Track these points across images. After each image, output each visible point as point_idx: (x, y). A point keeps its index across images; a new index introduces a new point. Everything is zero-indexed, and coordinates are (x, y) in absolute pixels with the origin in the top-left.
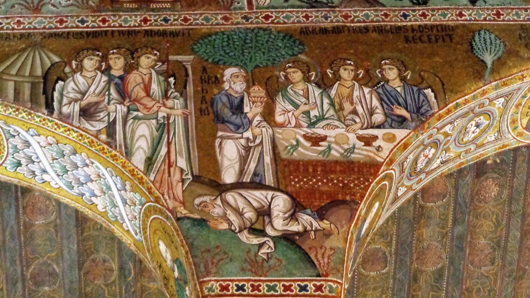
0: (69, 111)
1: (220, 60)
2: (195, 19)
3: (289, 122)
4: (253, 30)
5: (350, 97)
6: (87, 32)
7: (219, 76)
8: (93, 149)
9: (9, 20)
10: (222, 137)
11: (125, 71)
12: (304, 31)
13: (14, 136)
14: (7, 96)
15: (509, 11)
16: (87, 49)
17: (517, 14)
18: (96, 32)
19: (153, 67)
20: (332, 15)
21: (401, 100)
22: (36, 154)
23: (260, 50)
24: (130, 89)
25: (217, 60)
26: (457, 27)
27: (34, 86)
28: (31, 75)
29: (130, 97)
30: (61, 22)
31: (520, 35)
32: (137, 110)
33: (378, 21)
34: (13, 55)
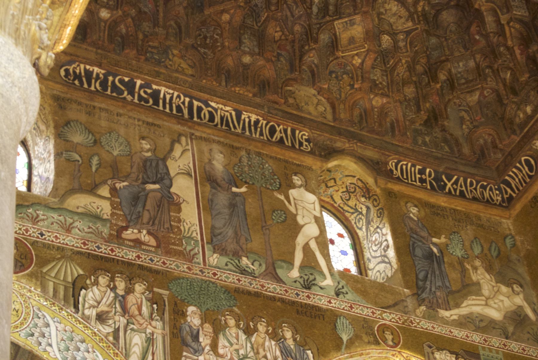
0: (89, 313)
1: (185, 299)
2: (170, 264)
3: (227, 355)
4: (206, 282)
5: (263, 345)
6: (101, 256)
7: (184, 310)
8: (101, 344)
9: (50, 234)
10: (185, 356)
11: (125, 292)
12: (237, 291)
13: (39, 318)
14: (48, 292)
15: (358, 306)
16: (101, 269)
17: (362, 310)
18: (107, 257)
19: (143, 293)
20: (253, 282)
21: (293, 355)
22: (50, 333)
23: (210, 297)
24: (129, 306)
25: (183, 298)
26: (327, 310)
27: (66, 288)
28: (64, 280)
29: (129, 313)
30: (84, 244)
31: (363, 325)
32: (133, 324)
33: (281, 294)
34: (54, 261)
